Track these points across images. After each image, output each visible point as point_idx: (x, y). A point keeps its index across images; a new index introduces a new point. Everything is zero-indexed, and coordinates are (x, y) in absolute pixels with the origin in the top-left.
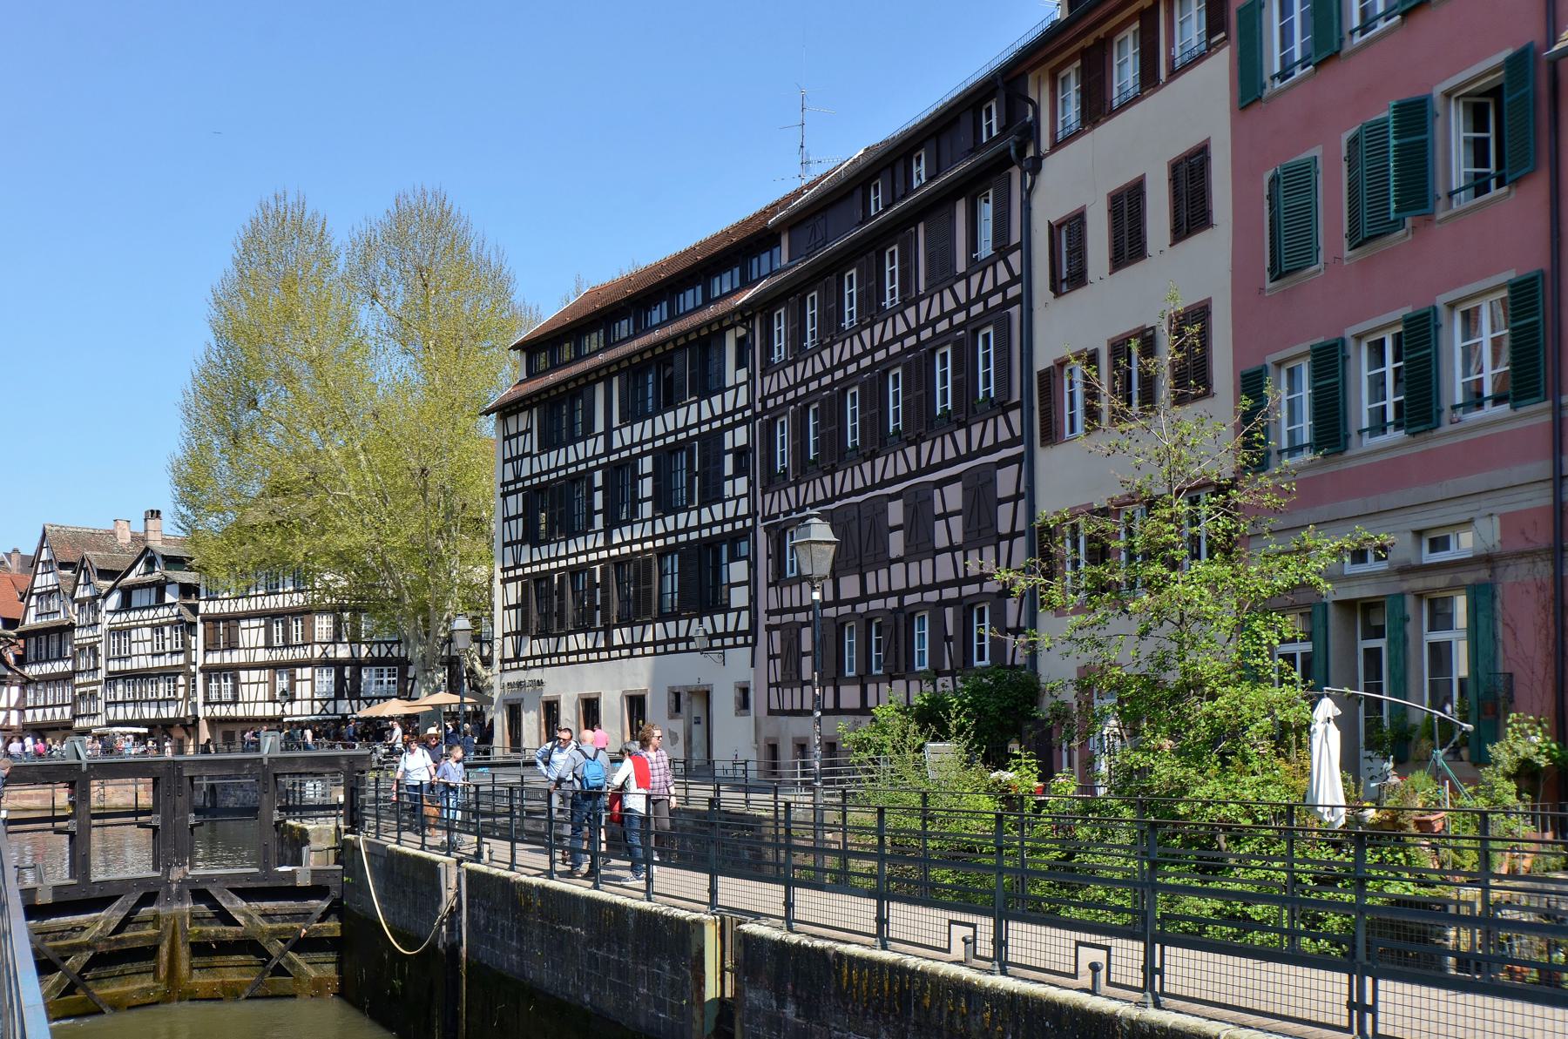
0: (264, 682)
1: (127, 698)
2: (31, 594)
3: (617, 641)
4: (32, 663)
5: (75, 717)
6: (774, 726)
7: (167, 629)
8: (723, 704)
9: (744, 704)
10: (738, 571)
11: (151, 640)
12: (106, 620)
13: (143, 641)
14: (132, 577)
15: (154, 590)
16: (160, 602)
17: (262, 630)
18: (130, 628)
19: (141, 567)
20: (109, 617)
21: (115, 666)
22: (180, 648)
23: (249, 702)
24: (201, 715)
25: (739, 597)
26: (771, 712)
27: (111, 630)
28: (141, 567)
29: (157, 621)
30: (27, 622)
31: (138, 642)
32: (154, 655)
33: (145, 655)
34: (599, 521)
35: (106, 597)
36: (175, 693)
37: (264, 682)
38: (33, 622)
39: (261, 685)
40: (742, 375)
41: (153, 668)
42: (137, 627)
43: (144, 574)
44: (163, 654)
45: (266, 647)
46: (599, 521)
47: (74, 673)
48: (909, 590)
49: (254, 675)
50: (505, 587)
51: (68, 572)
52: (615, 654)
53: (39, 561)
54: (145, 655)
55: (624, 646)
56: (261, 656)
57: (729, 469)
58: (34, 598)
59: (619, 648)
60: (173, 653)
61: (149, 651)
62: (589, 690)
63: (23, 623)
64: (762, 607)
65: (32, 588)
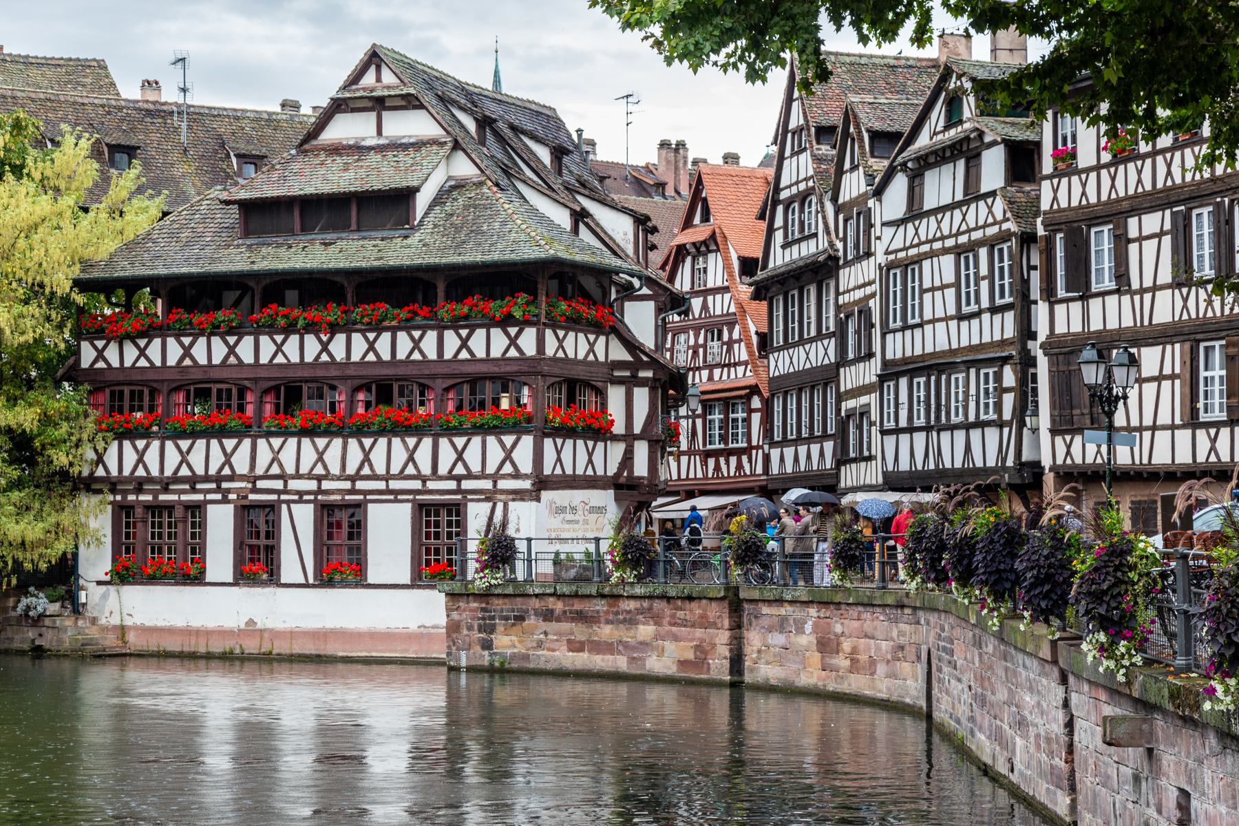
0: (1172, 377)
1: (917, 423)
2: (776, 202)
4: (779, 349)
5: (842, 460)
7: (983, 252)
11: (957, 284)
12: (886, 242)
13: (943, 287)
14: (923, 141)
15: (961, 164)
16: (973, 195)
17: (1167, 240)
18: (918, 260)
19: (938, 115)
20: (888, 232)
21: (897, 347)
22: (1008, 299)
23: (1141, 429)
24: (1046, 462)
27: (890, 266)
28: (938, 115)
29: (963, 239)
30: (771, 265)
31: (933, 289)
32: (960, 317)
33: (947, 319)
35: (878, 193)
36: (999, 407)
37: (1172, 377)
38: (779, 262)
39: (1166, 385)
41: (960, 350)
42: (931, 255)
43: (947, 128)
44: (977, 314)
45: (1176, 285)
47: (842, 361)
51: (825, 150)
53: (786, 131)
54: (947, 319)
58: (780, 209)
60: (994, 310)
61: (952, 311)
63: (765, 267)
65: (777, 189)
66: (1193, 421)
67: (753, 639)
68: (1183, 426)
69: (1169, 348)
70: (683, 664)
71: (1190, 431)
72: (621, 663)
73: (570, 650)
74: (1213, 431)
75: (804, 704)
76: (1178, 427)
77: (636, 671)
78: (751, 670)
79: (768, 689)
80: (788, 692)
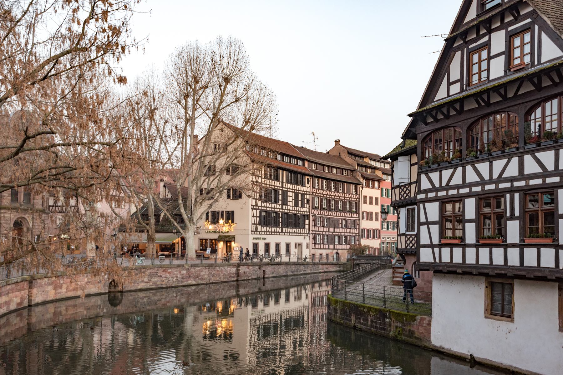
3: (284, 231)
6: (314, 251)
8: (304, 246)
9: (307, 247)
10: (307, 222)
25: (307, 227)
26: (312, 248)
34: (280, 202)
40: (308, 186)
46: (280, 202)
48: (342, 233)
50: (252, 210)
52: (283, 234)
55: (286, 232)
57: (306, 202)
59: (285, 233)
62: (278, 242)
64: (311, 229)
78: (34, 300)
80: (44, 303)
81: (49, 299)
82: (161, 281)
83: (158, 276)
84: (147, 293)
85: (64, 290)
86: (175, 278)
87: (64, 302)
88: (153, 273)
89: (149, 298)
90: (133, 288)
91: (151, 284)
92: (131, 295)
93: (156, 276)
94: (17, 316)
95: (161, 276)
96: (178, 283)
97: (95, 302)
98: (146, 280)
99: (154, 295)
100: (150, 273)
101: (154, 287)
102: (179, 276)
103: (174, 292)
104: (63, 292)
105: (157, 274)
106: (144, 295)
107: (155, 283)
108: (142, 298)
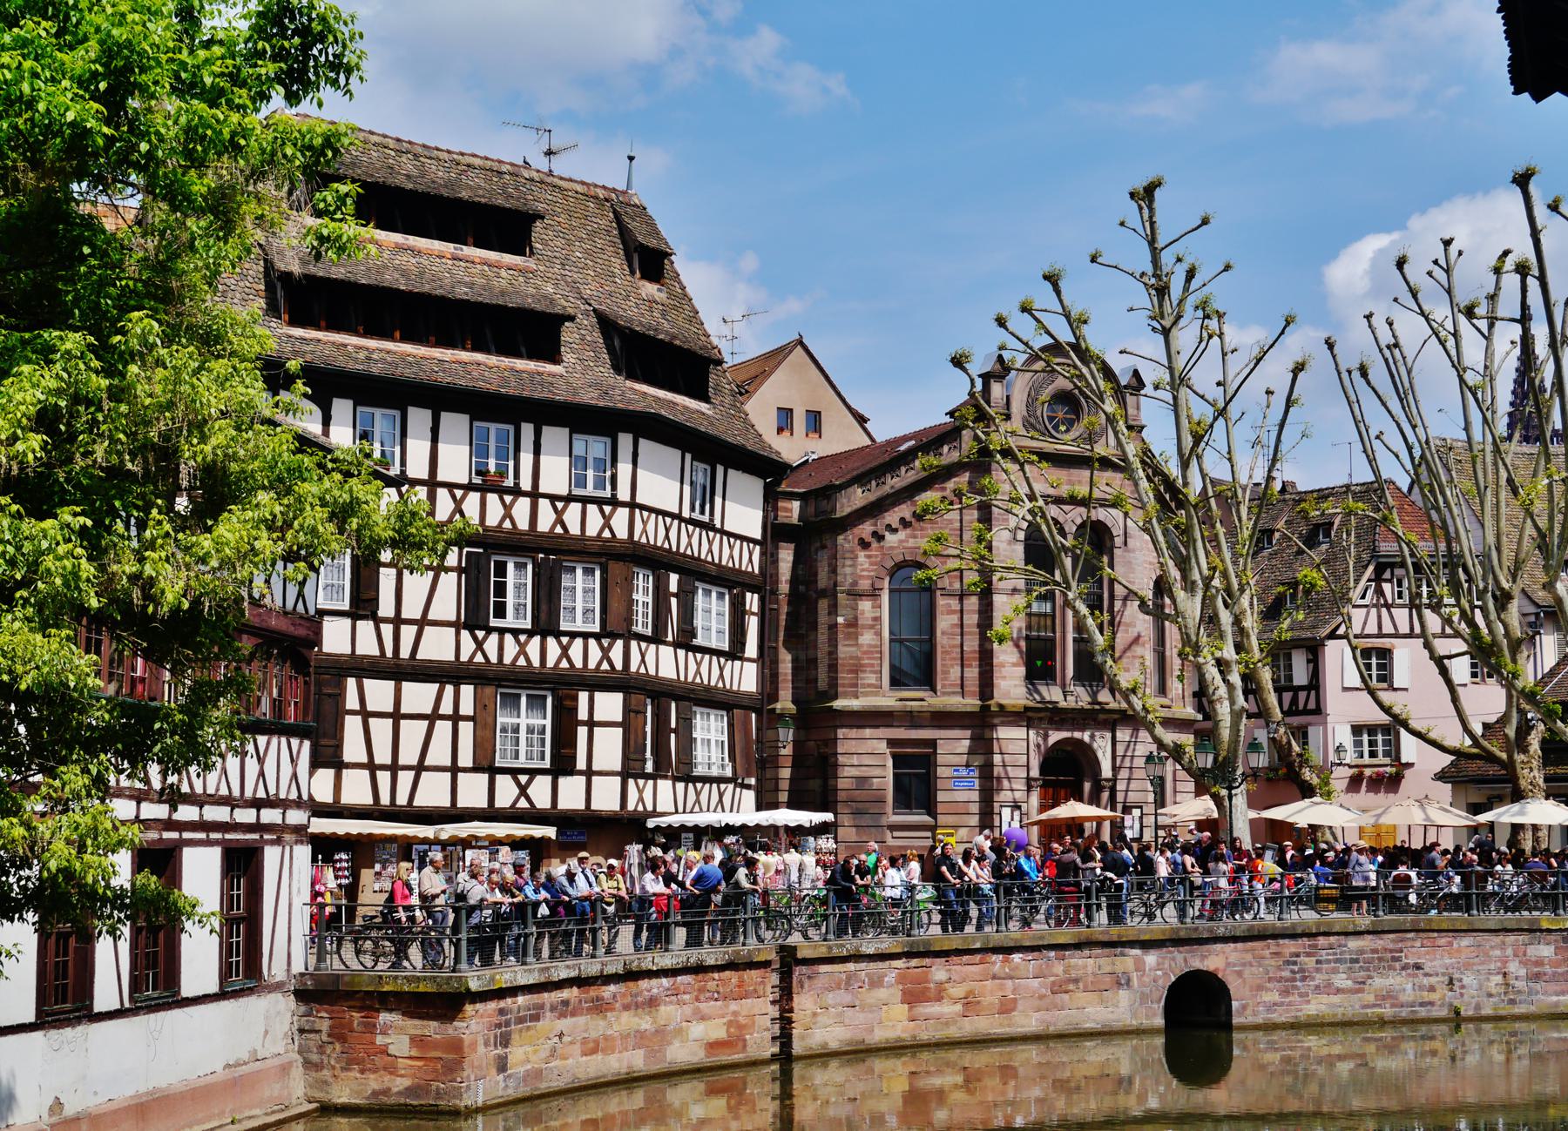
45: (457, 625)
49: (419, 696)
56: (438, 646)
66: (486, 765)
67: (803, 1003)
68: (476, 769)
69: (449, 689)
70: (713, 1046)
71: (485, 777)
72: (636, 1060)
73: (585, 1054)
74: (523, 779)
75: (879, 1064)
76: (465, 770)
77: (655, 1068)
78: (803, 1038)
79: (823, 1056)
80: (857, 1053)
81: (879, 1036)
82: (1421, 988)
83: (1404, 968)
84: (1352, 1042)
85: (947, 1009)
86: (1499, 979)
87: (953, 1055)
88: (1374, 951)
89: (1363, 1061)
90: (1279, 1017)
91: (1370, 998)
92: (1272, 1047)
93: (1391, 968)
94: (712, 1091)
95: (1418, 967)
96: (1512, 1002)
97: (1103, 1065)
98: (1341, 981)
99: (1391, 1049)
100: (1362, 952)
101: (1387, 1011)
102: (1514, 967)
103: (1491, 1042)
104: (944, 1017)
105: (1398, 959)
106: (1337, 1050)
107: (1388, 996)
108: (1330, 1061)
